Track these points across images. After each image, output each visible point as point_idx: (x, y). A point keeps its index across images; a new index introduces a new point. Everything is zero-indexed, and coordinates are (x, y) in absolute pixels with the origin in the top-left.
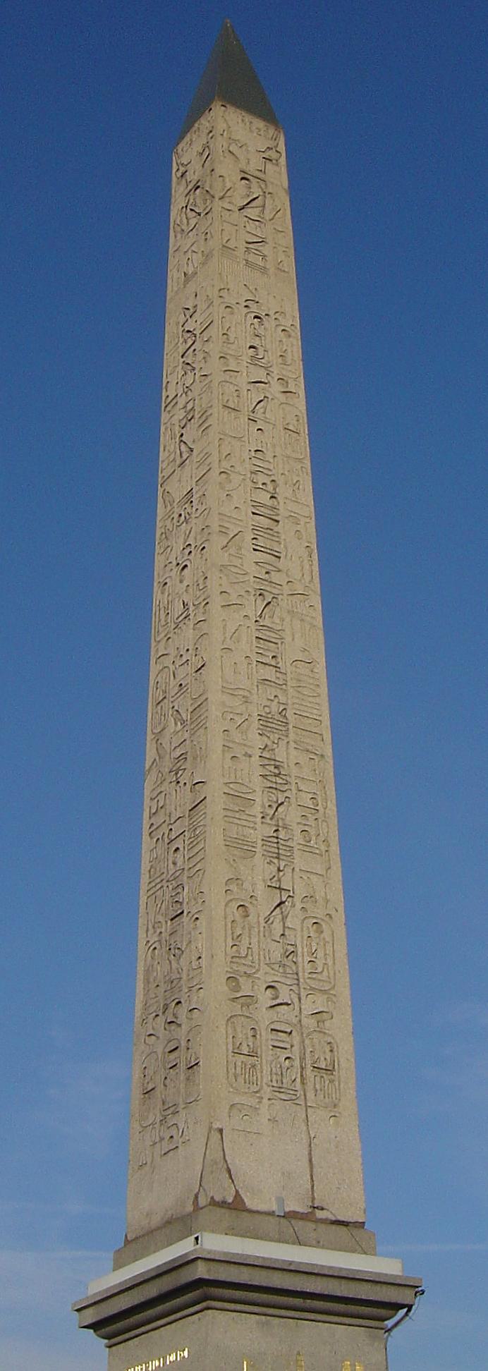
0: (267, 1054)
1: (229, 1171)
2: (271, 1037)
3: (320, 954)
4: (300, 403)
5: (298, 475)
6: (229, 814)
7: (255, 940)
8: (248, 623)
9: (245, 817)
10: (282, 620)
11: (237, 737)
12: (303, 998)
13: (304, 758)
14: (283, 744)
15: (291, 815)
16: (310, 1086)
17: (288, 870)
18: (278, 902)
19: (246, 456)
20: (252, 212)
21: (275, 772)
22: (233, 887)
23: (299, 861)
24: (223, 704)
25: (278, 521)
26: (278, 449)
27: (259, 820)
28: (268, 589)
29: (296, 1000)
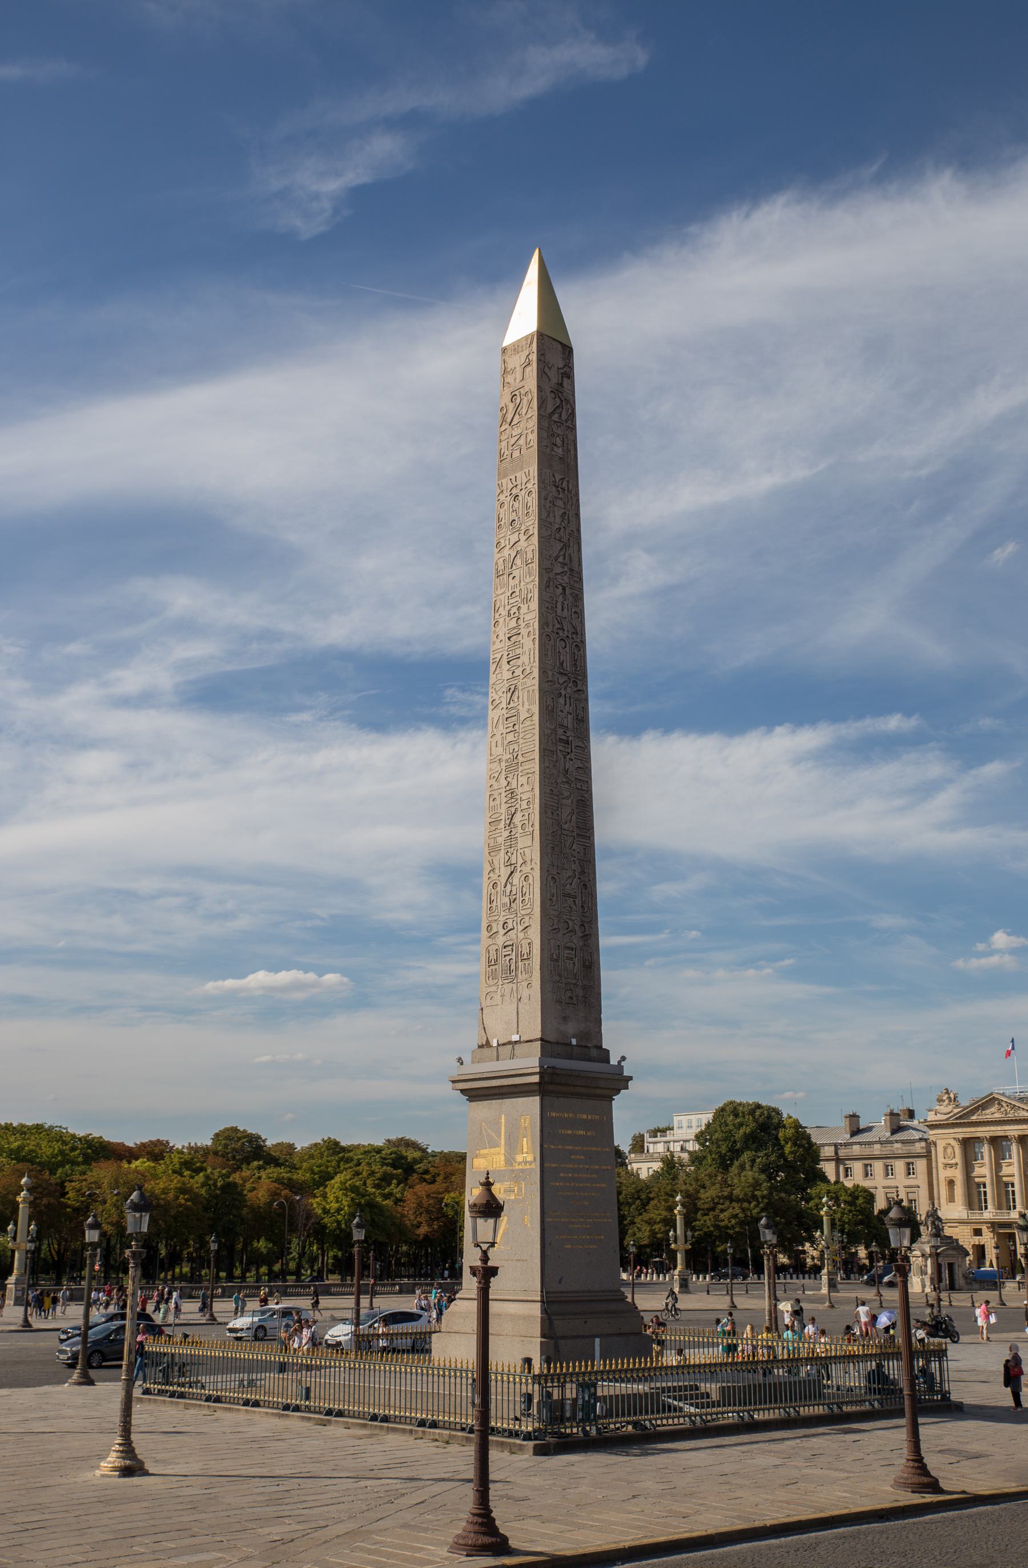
3: (527, 894)
4: (535, 540)
9: (497, 831)
10: (518, 698)
11: (496, 786)
14: (516, 777)
15: (518, 819)
19: (506, 601)
22: (491, 875)
23: (520, 845)
26: (522, 583)
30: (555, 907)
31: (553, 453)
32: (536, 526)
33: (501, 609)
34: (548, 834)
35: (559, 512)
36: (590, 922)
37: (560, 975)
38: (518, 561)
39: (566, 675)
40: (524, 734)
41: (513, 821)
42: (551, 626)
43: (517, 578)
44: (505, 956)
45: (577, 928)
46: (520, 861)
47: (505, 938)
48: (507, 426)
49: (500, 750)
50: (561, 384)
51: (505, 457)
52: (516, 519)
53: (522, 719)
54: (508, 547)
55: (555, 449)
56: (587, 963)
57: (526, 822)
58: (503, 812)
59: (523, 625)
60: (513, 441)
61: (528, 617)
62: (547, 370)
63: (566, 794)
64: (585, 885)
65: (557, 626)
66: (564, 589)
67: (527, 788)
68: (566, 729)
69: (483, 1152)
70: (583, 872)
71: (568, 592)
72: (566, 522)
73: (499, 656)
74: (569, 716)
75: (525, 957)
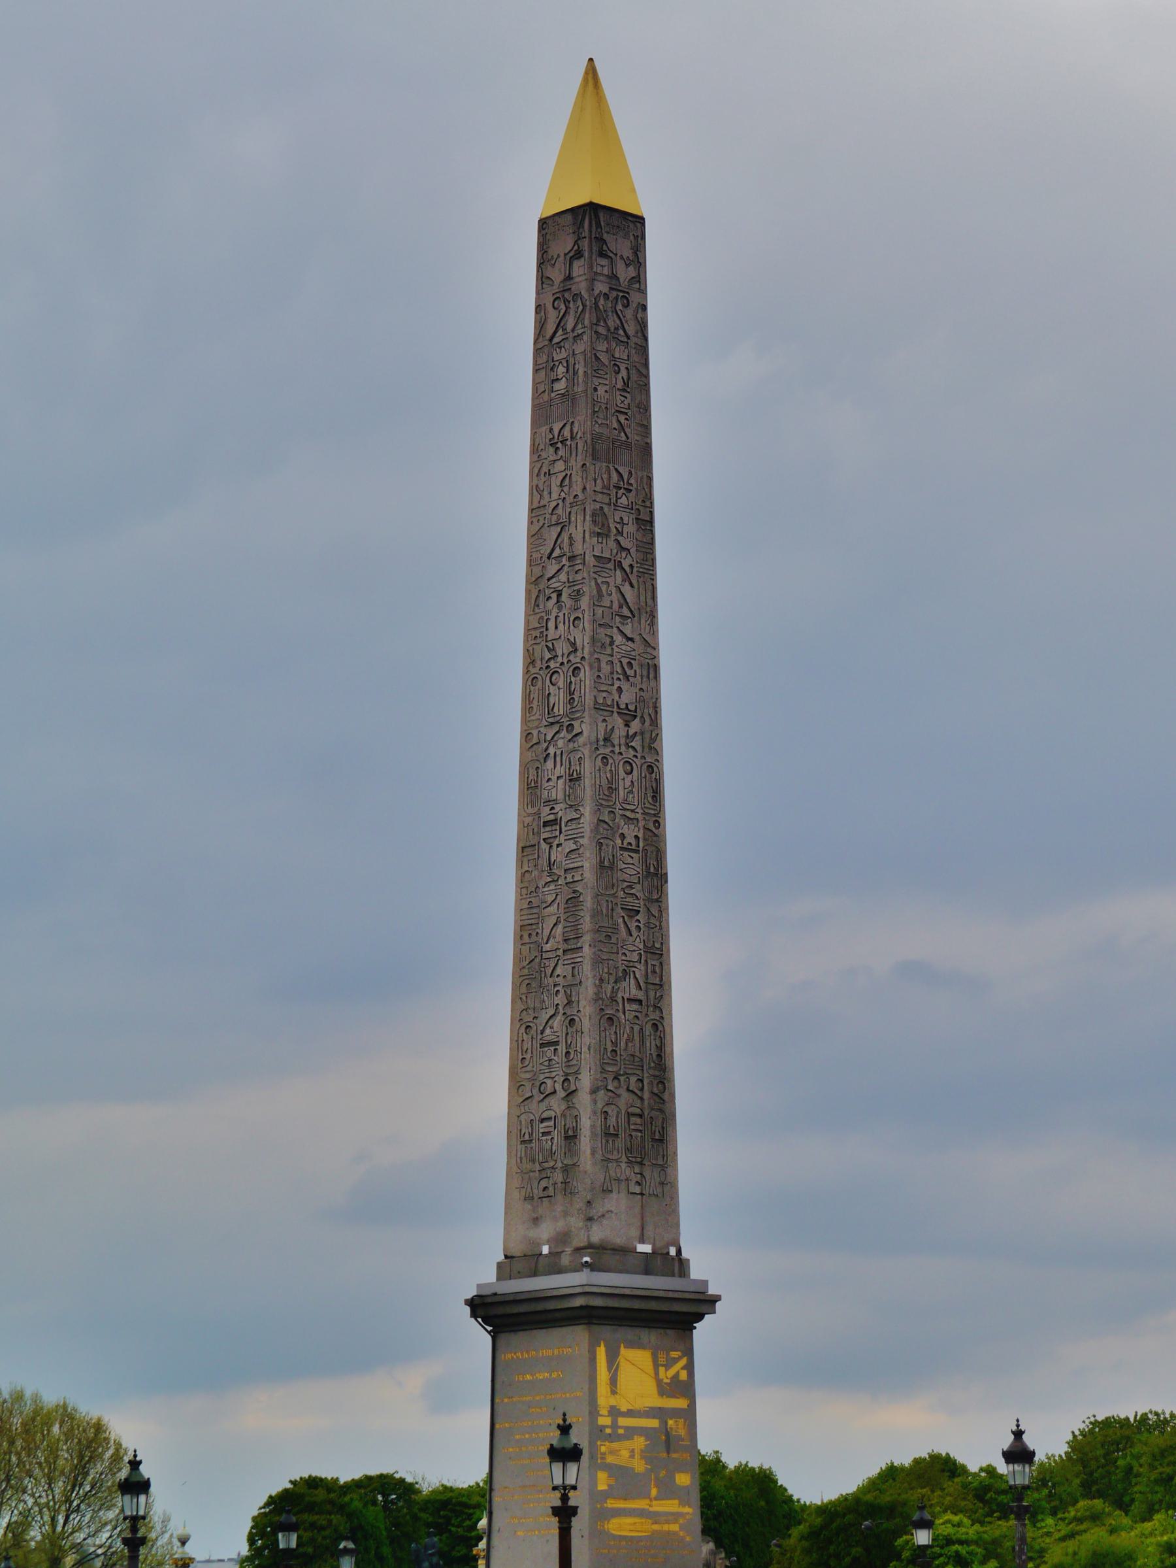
30: (529, 1068)
31: (553, 395)
34: (524, 967)
35: (555, 481)
36: (577, 1073)
37: (533, 1161)
39: (557, 722)
42: (538, 664)
45: (558, 1087)
50: (569, 278)
55: (557, 386)
56: (570, 1133)
62: (551, 272)
63: (550, 898)
64: (572, 1021)
65: (547, 656)
66: (559, 595)
68: (551, 803)
70: (569, 1003)
71: (564, 597)
72: (566, 489)
74: (561, 782)
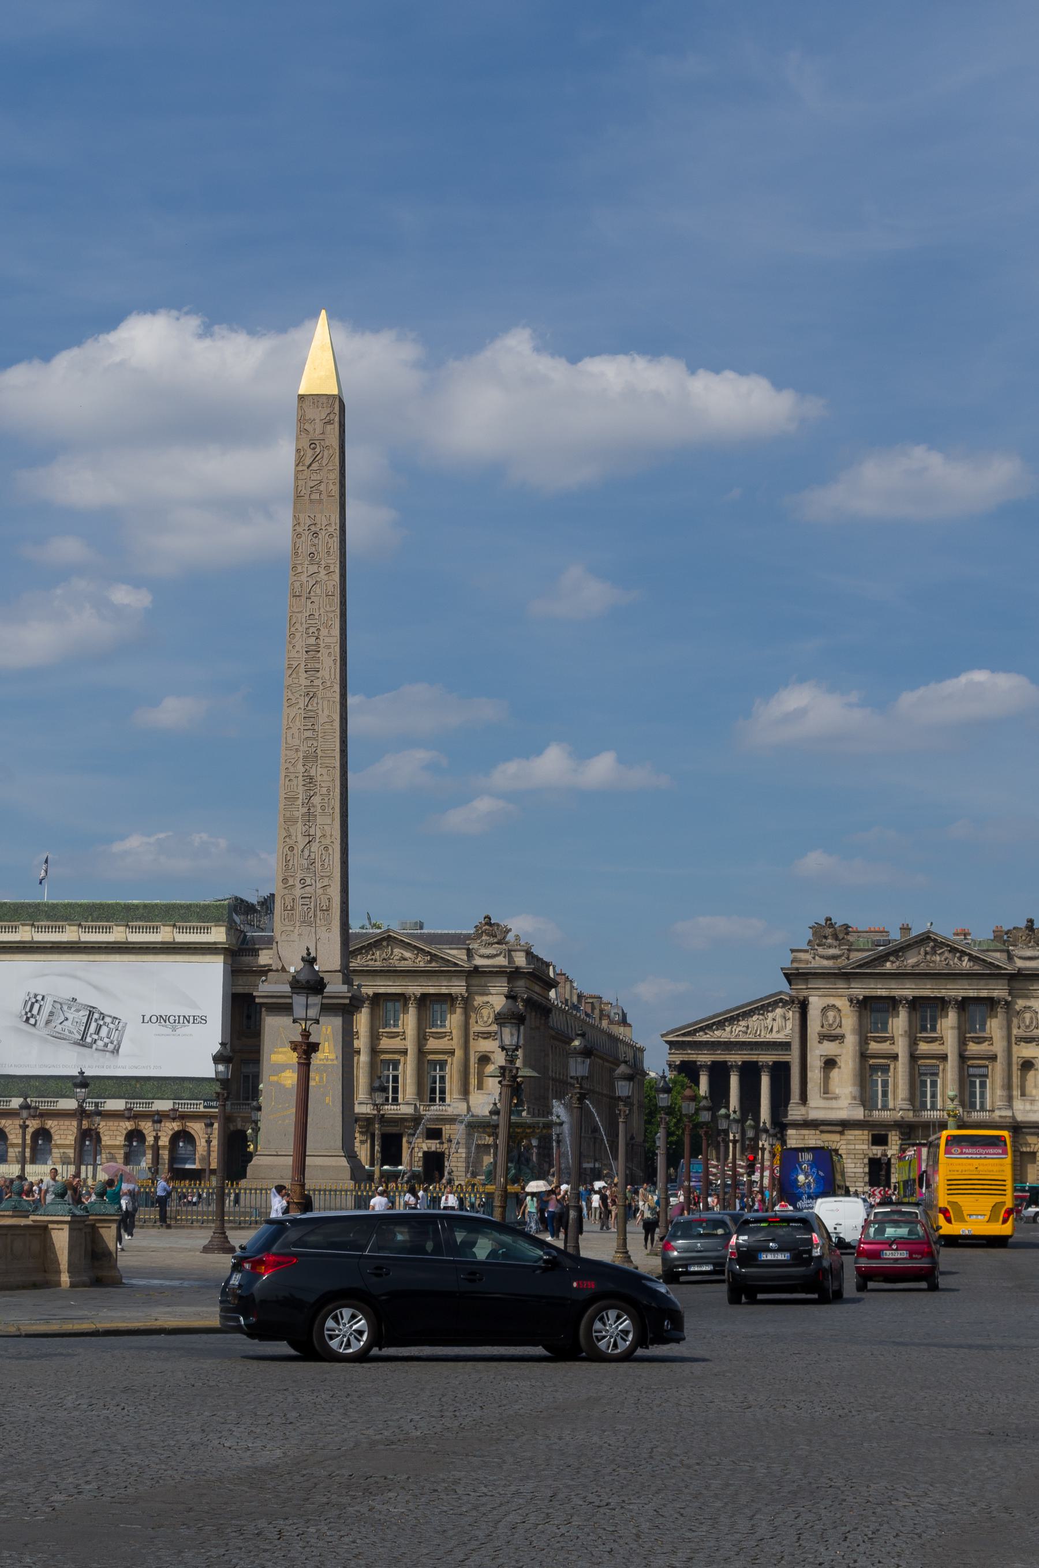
0: (299, 908)
1: (280, 958)
2: (301, 900)
3: (327, 860)
5: (331, 621)
6: (287, 807)
7: (296, 861)
8: (300, 711)
10: (317, 703)
11: (292, 770)
12: (317, 881)
13: (324, 771)
14: (314, 767)
15: (316, 800)
16: (318, 918)
17: (313, 826)
18: (307, 841)
19: (304, 620)
20: (315, 466)
21: (310, 780)
22: (287, 840)
23: (319, 820)
24: (286, 755)
25: (319, 651)
26: (322, 610)
27: (301, 806)
28: (311, 690)
29: (314, 883)
32: (338, 566)
33: (297, 626)
38: (318, 590)
40: (323, 734)
41: (311, 801)
43: (317, 603)
44: (302, 905)
46: (319, 834)
47: (303, 891)
48: (305, 468)
49: (297, 742)
51: (302, 494)
52: (316, 553)
53: (321, 721)
54: (305, 575)
57: (326, 805)
58: (301, 792)
59: (322, 645)
60: (312, 484)
61: (328, 640)
67: (325, 778)
69: (280, 1050)
73: (295, 664)
75: (324, 908)
